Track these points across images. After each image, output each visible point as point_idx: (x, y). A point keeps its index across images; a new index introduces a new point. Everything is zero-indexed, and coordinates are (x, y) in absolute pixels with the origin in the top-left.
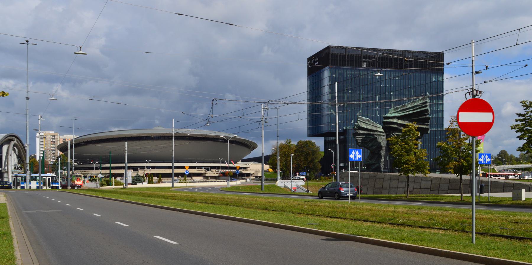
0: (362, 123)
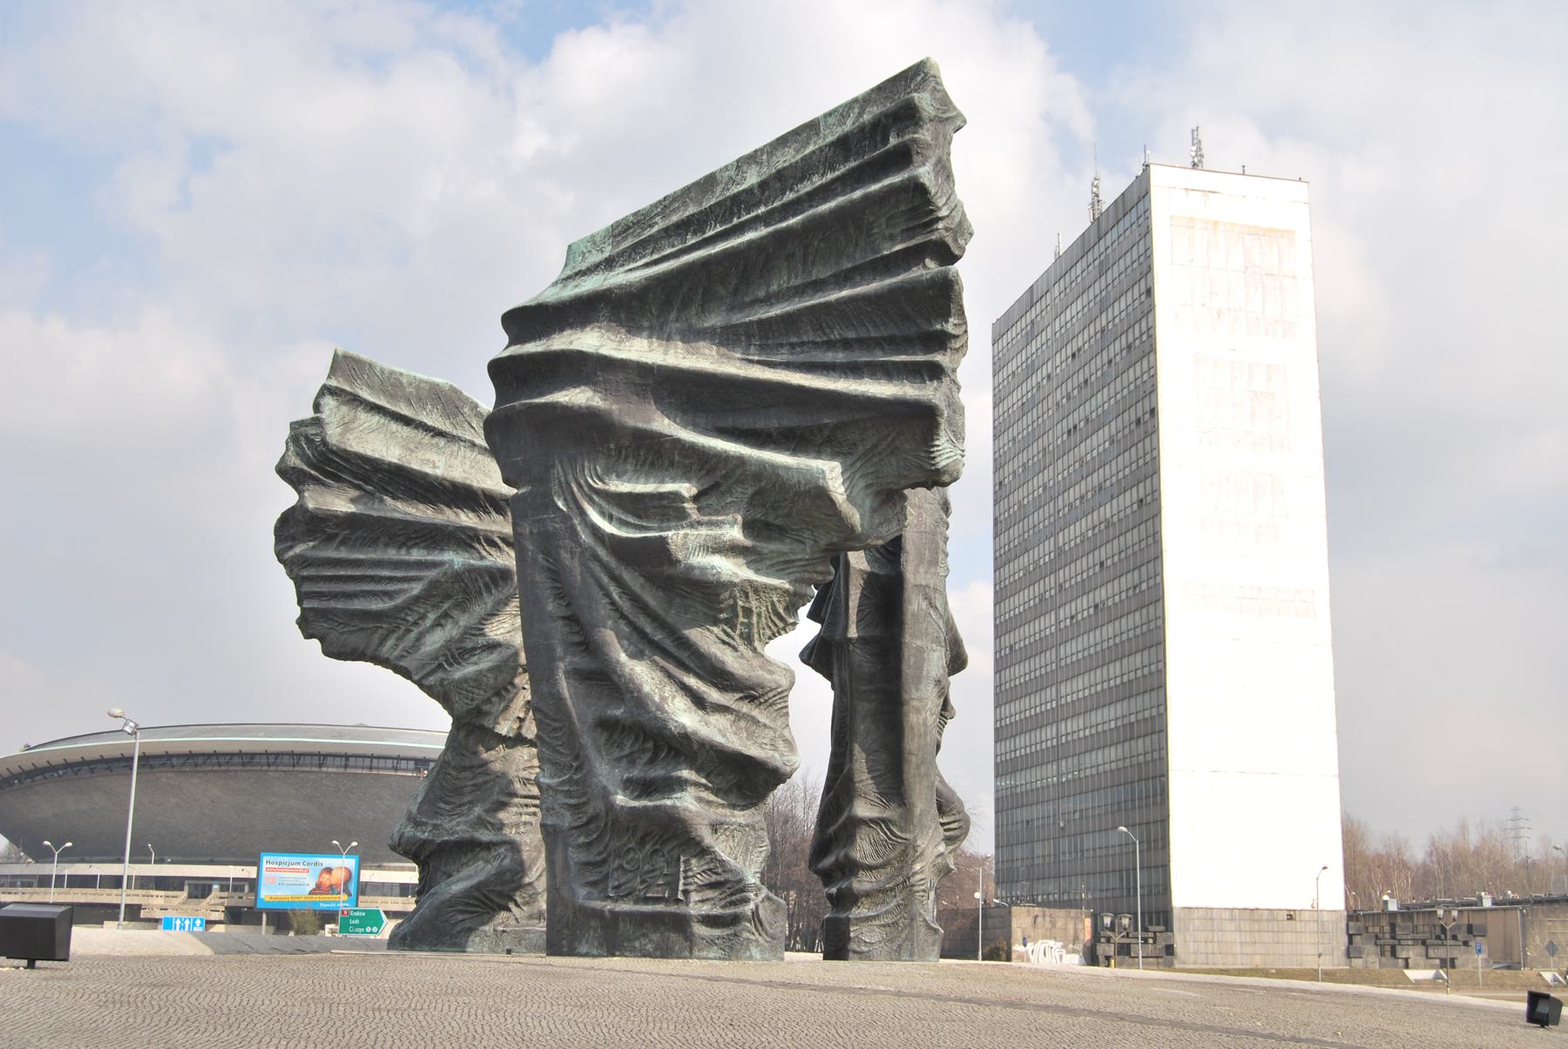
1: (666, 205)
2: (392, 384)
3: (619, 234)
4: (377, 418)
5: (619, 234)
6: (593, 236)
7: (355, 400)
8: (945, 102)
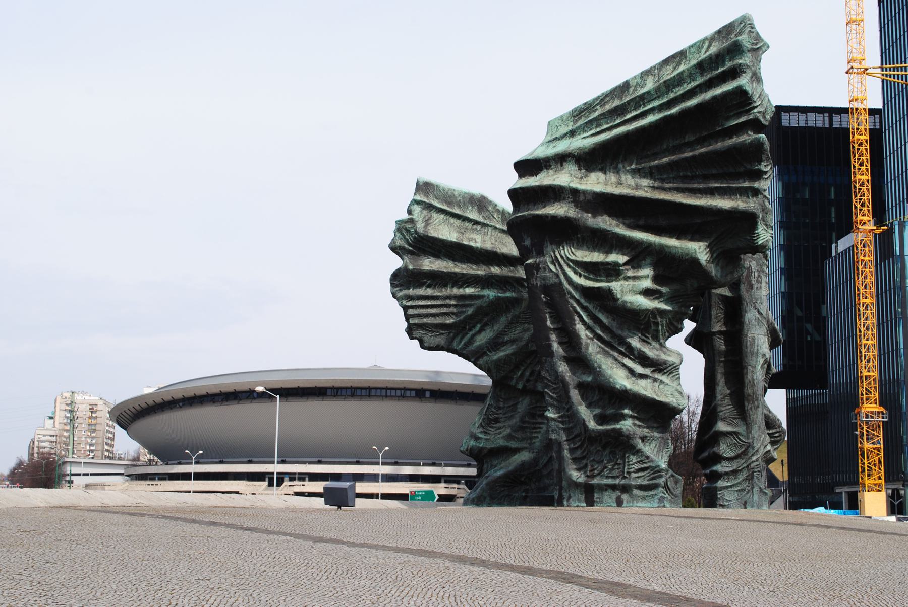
0: (438, 218)
1: (603, 100)
2: (448, 197)
3: (577, 116)
4: (443, 216)
5: (577, 116)
6: (562, 117)
7: (429, 207)
8: (758, 38)
